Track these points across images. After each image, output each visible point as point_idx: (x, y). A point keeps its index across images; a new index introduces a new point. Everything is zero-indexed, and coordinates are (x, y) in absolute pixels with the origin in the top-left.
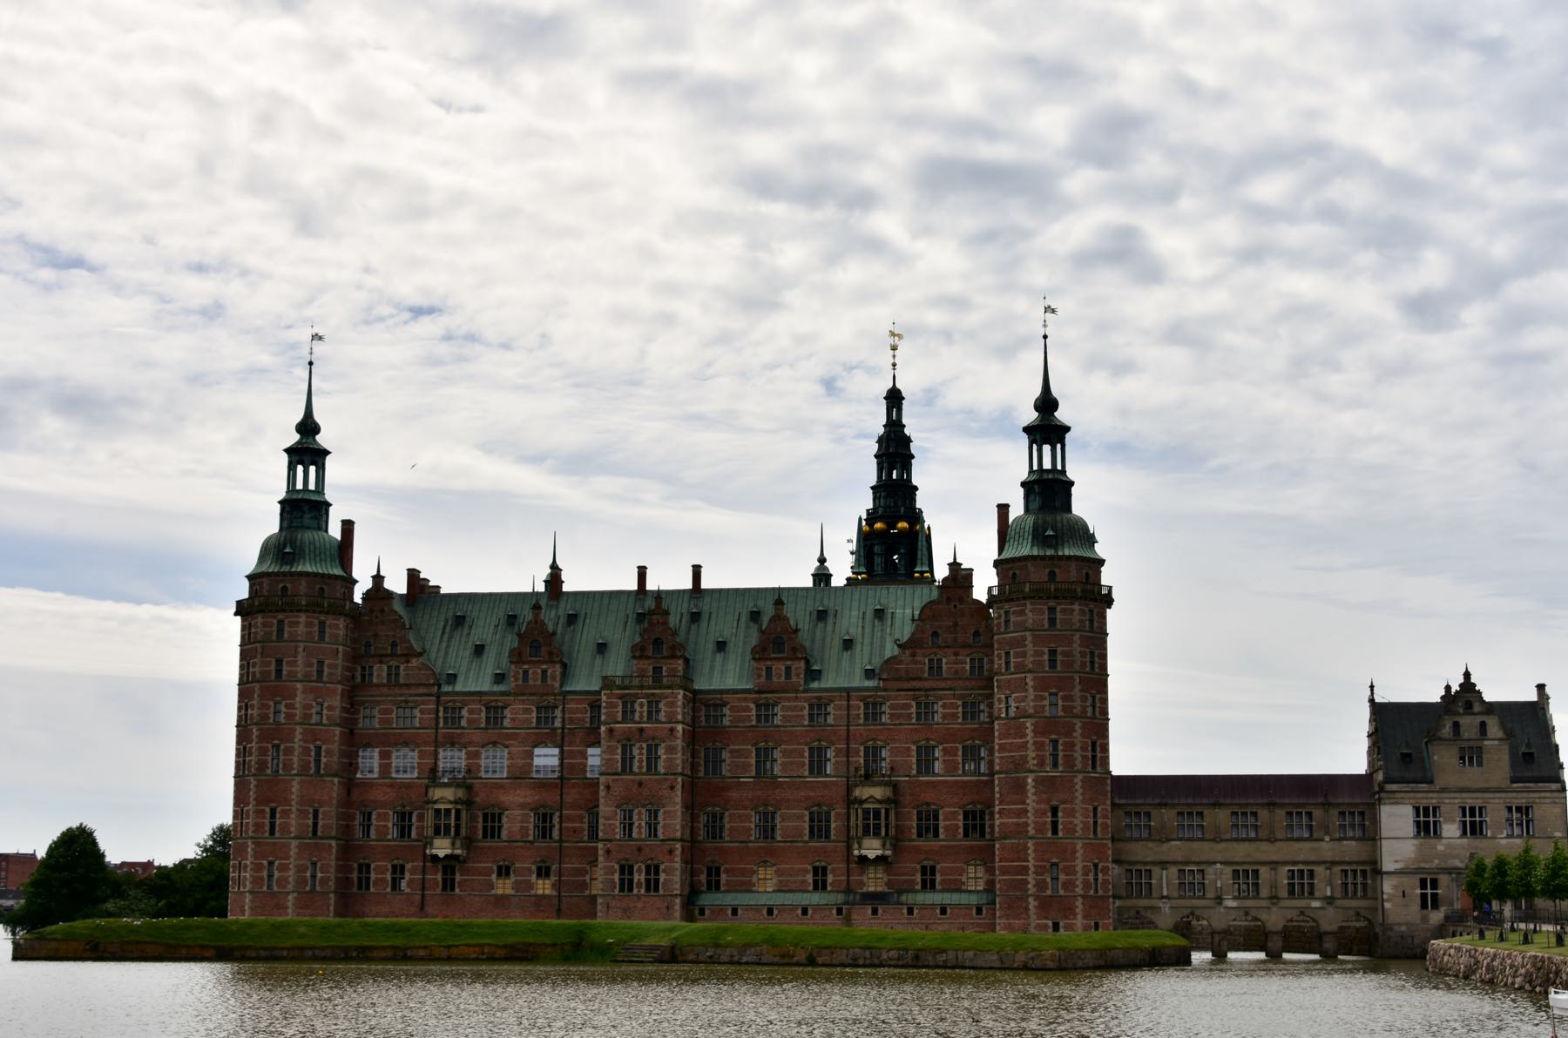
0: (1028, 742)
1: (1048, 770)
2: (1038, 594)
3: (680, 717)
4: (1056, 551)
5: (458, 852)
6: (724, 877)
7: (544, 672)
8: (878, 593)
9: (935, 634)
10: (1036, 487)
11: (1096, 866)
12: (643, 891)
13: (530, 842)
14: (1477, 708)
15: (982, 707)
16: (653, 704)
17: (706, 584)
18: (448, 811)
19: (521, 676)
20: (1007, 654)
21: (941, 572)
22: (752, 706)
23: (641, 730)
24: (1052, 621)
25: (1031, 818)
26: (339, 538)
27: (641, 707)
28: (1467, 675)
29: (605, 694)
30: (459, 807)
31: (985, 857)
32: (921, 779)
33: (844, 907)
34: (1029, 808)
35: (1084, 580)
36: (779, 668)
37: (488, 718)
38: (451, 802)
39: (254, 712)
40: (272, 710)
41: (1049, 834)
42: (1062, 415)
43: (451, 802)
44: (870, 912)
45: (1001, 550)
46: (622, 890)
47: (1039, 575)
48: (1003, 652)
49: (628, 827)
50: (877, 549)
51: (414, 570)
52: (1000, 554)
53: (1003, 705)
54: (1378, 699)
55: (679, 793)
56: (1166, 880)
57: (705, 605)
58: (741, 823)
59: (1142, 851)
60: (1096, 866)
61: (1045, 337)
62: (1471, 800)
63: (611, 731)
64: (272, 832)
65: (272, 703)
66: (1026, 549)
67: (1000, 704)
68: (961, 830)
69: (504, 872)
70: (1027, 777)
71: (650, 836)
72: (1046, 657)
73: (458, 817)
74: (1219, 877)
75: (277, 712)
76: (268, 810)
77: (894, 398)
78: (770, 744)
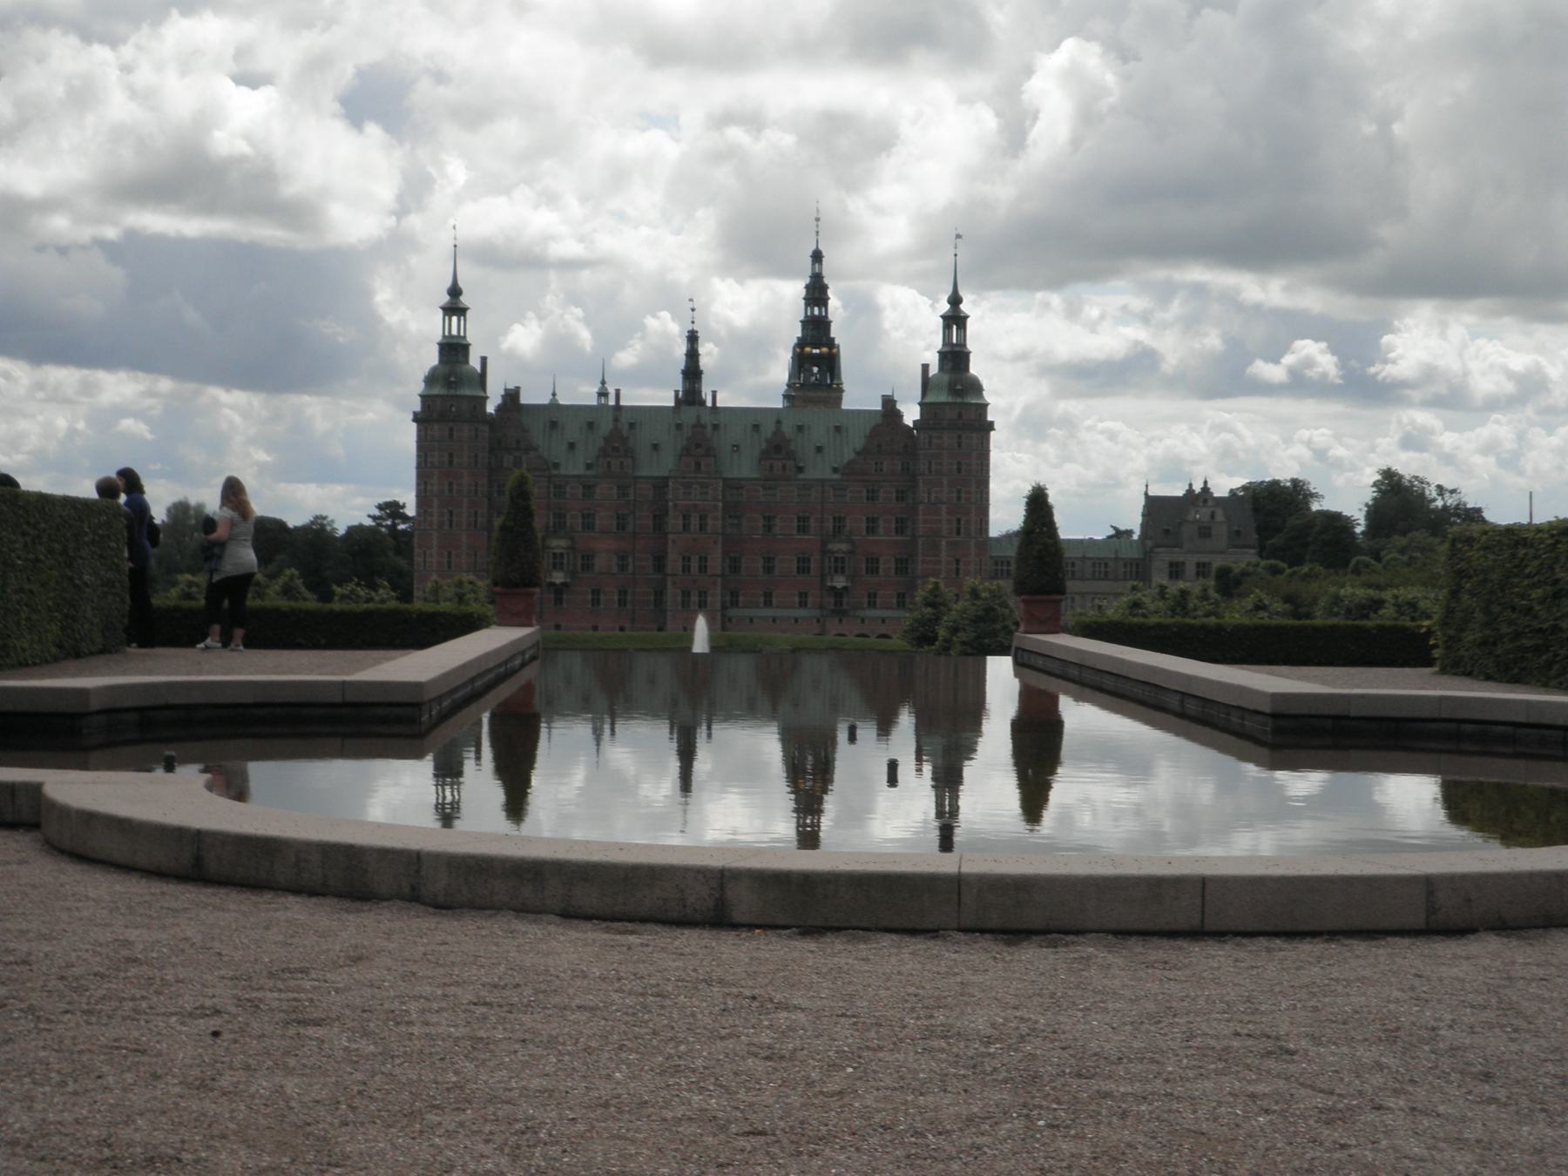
3: (720, 497)
5: (568, 580)
6: (741, 598)
7: (622, 463)
9: (879, 446)
10: (949, 356)
14: (1210, 503)
17: (718, 405)
18: (562, 555)
20: (930, 463)
22: (761, 489)
23: (695, 505)
24: (959, 445)
26: (478, 368)
28: (1206, 482)
37: (584, 495)
49: (686, 569)
50: (806, 366)
53: (926, 495)
54: (1150, 494)
61: (956, 255)
63: (676, 505)
64: (449, 567)
66: (943, 398)
72: (955, 467)
75: (451, 490)
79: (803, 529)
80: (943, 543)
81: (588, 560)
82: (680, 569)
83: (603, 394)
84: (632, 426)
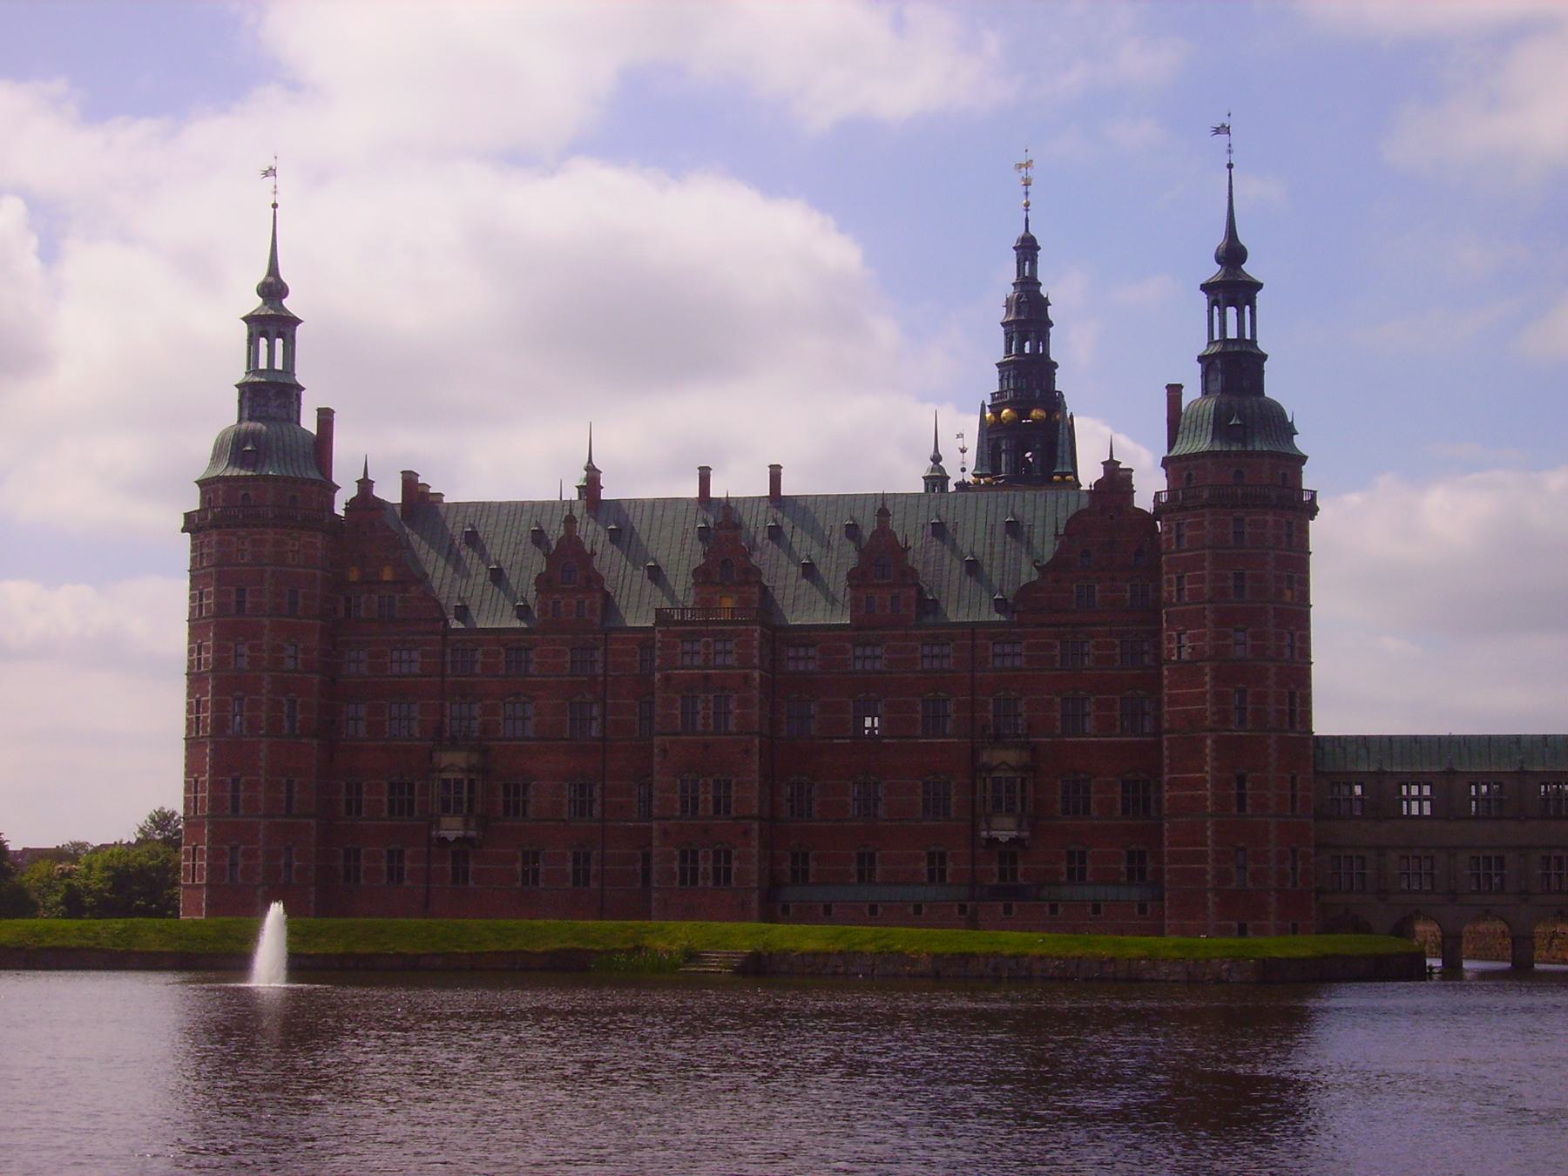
0: (1207, 692)
1: (1234, 728)
3: (756, 661)
4: (1245, 445)
5: (472, 833)
6: (813, 866)
8: (1062, 500)
10: (1218, 362)
11: (1294, 851)
12: (710, 884)
13: (564, 820)
15: (1146, 648)
18: (459, 782)
19: (550, 608)
20: (1180, 578)
21: (1089, 473)
22: (849, 646)
23: (707, 677)
25: (1209, 792)
26: (315, 432)
29: (659, 632)
30: (473, 776)
32: (1067, 739)
33: (968, 904)
34: (1208, 777)
35: (1280, 484)
38: (462, 770)
40: (232, 653)
41: (1235, 810)
42: (1250, 268)
43: (462, 770)
44: (1001, 909)
45: (1171, 444)
46: (683, 881)
48: (1174, 576)
51: (411, 472)
52: (1170, 450)
53: (1174, 645)
55: (756, 758)
60: (1294, 851)
63: (667, 678)
64: (235, 808)
65: (232, 644)
66: (1203, 444)
67: (1169, 643)
68: (1119, 806)
70: (1206, 737)
71: (717, 811)
72: (1231, 583)
73: (471, 789)
76: (229, 780)
77: (1027, 249)
78: (872, 695)
80: (1209, 742)
82: (678, 806)
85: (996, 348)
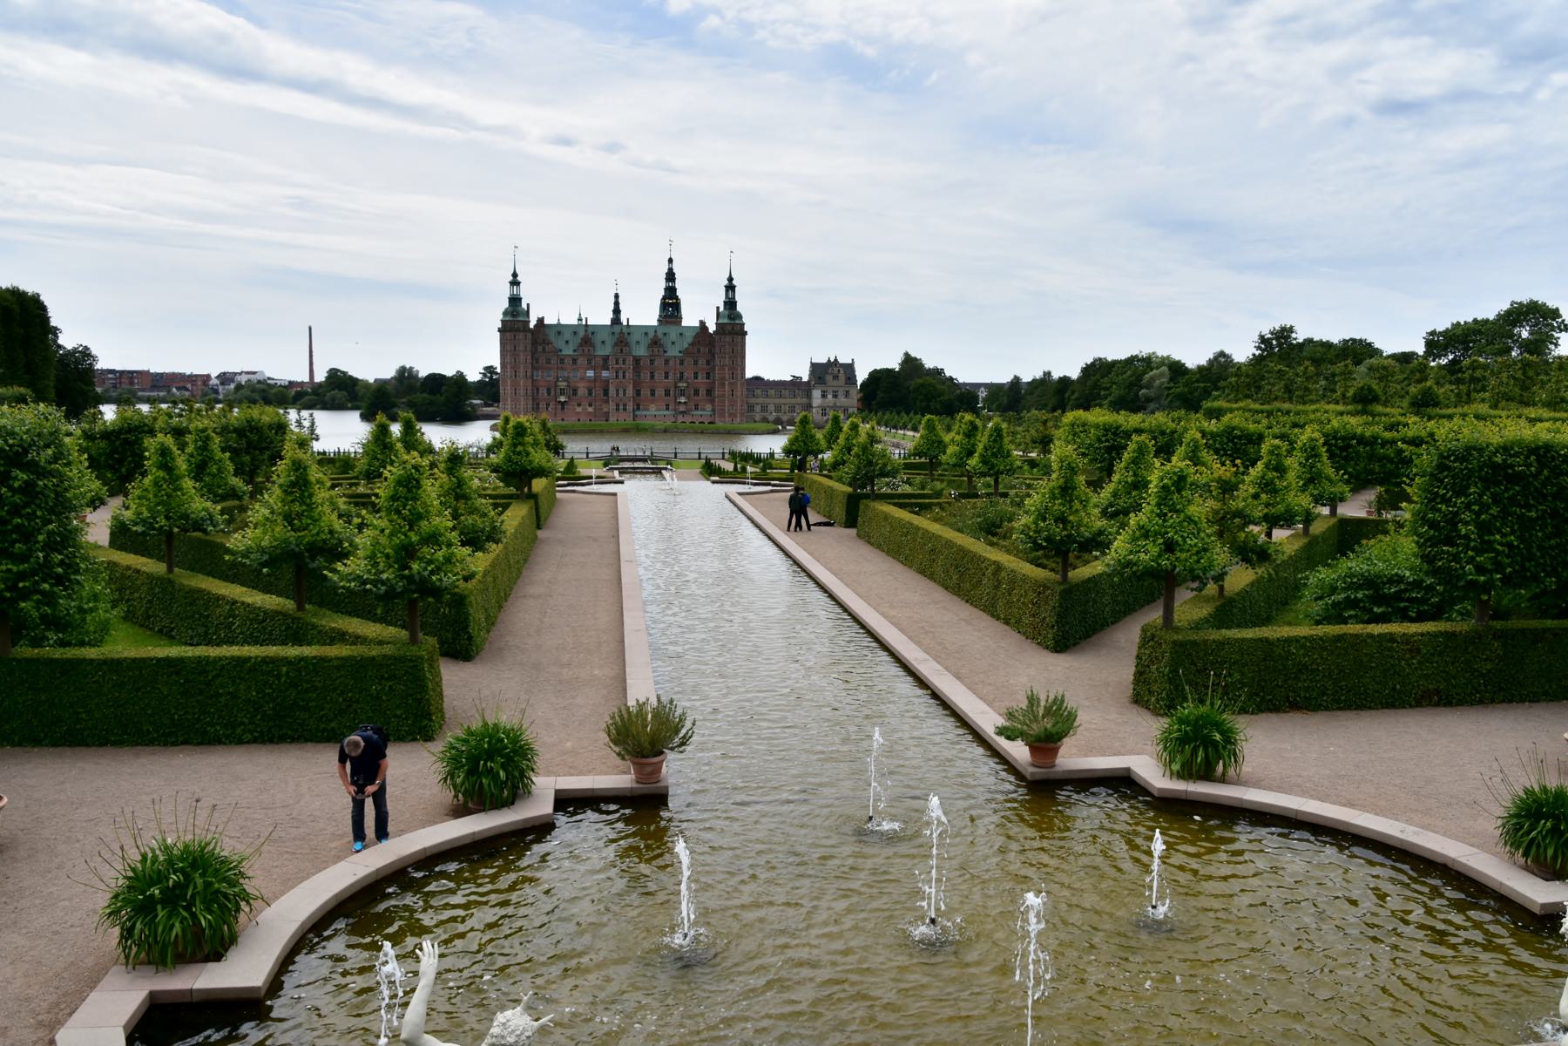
2: (730, 333)
16: (624, 361)
27: (621, 361)
31: (712, 402)
36: (656, 350)
39: (508, 360)
47: (729, 328)
49: (617, 395)
56: (758, 408)
57: (632, 330)
58: (646, 392)
59: (752, 401)
62: (835, 389)
69: (579, 405)
74: (771, 408)
77: (670, 261)
79: (666, 377)
81: (575, 391)
83: (580, 319)
84: (593, 333)
85: (663, 284)
